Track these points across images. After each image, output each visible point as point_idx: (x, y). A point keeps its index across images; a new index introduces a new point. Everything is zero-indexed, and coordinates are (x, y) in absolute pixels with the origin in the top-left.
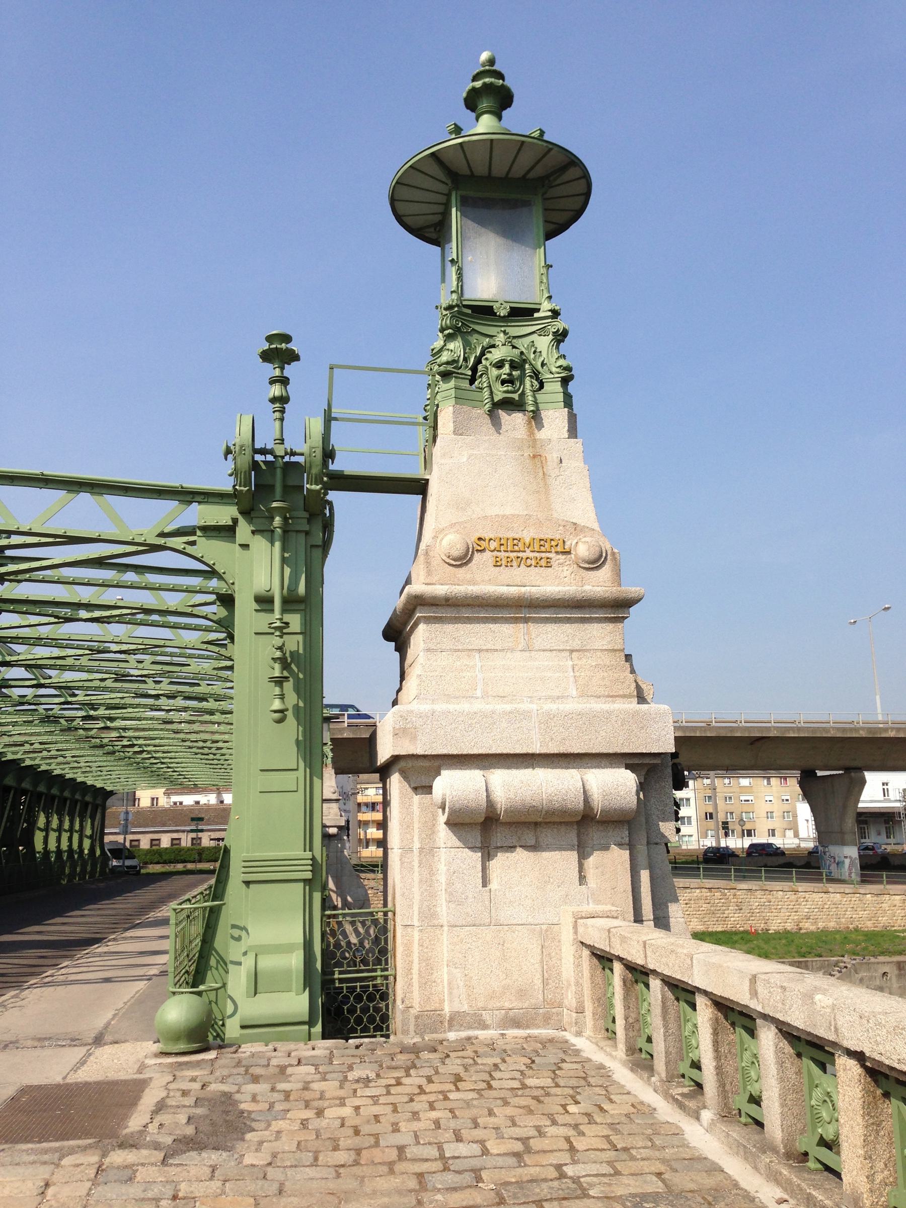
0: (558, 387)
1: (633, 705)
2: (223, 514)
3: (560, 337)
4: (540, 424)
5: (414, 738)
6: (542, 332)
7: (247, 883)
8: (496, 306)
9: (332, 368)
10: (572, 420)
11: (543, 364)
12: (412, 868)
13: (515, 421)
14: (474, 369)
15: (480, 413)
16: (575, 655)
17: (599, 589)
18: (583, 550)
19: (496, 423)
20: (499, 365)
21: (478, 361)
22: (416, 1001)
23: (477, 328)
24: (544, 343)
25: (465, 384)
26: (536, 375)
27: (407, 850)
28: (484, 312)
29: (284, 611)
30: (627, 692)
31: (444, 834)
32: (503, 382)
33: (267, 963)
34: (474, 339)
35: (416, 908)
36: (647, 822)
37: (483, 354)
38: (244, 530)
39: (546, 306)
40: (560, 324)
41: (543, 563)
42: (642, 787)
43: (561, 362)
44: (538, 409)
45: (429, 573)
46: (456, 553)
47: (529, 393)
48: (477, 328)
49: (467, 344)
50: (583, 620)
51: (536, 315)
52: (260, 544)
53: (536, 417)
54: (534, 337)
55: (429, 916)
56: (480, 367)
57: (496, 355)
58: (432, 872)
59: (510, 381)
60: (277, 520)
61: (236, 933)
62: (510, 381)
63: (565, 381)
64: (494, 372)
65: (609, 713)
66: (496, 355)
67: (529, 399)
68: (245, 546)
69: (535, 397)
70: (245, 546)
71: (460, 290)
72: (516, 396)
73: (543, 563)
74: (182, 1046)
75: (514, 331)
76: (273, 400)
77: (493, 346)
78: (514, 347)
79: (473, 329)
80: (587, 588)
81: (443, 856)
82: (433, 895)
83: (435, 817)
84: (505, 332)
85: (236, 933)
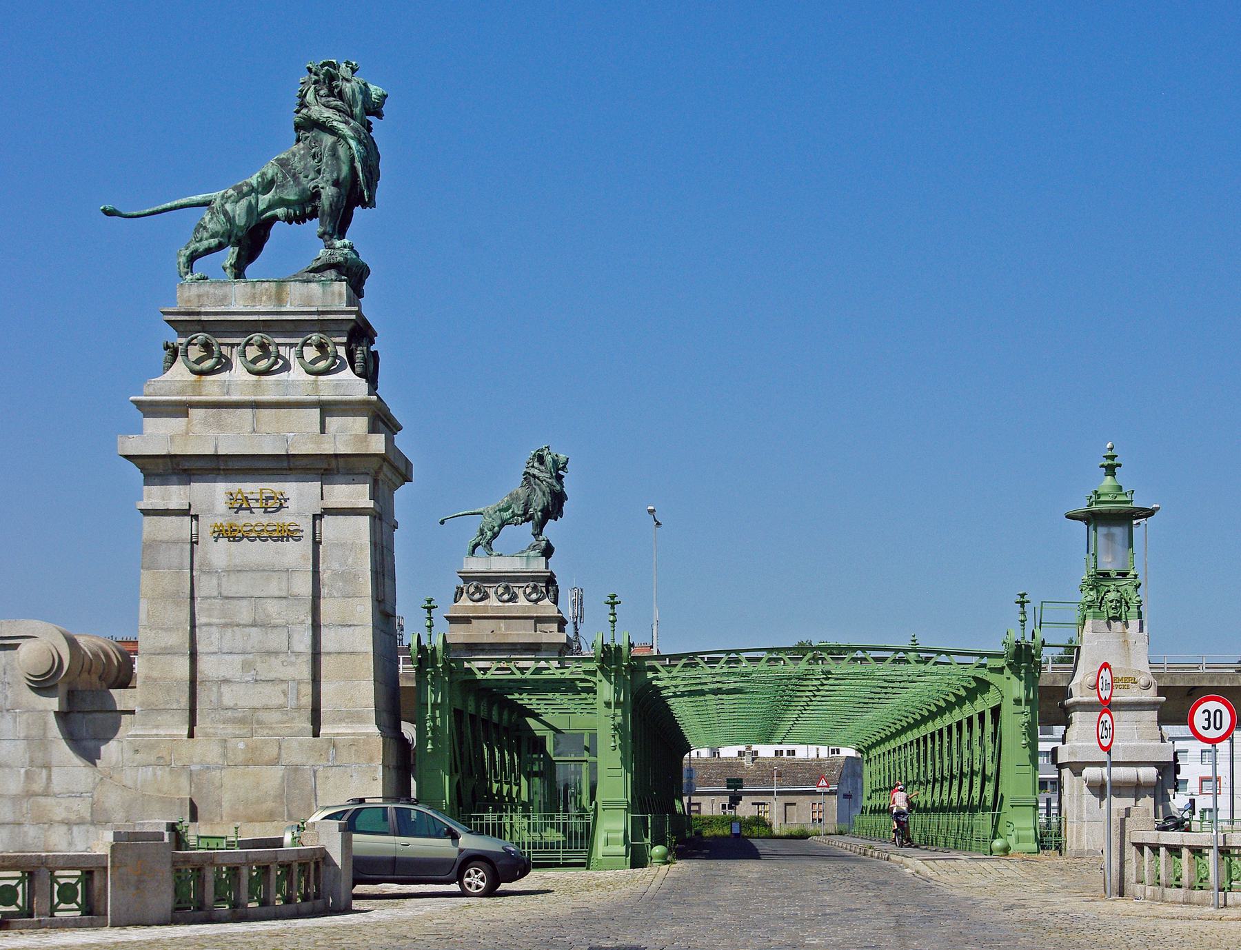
0: (1136, 610)
1: (1159, 743)
2: (1000, 663)
3: (1137, 587)
4: (1127, 627)
5: (1076, 756)
6: (1130, 584)
7: (1012, 806)
8: (1111, 572)
9: (1042, 603)
10: (1141, 624)
11: (1130, 599)
12: (1073, 802)
13: (1117, 626)
14: (1101, 603)
15: (1103, 622)
16: (1137, 723)
17: (1147, 698)
18: (1142, 682)
19: (1109, 626)
20: (1112, 601)
21: (1103, 599)
22: (1074, 847)
23: (1102, 583)
24: (1131, 589)
25: (1097, 610)
26: (1127, 603)
27: (1071, 795)
28: (1106, 575)
29: (1026, 705)
30: (1157, 738)
31: (1086, 789)
32: (1113, 609)
33: (1021, 833)
34: (1100, 589)
35: (1075, 816)
36: (1162, 788)
37: (1105, 595)
38: (1007, 672)
39: (1132, 572)
40: (1138, 581)
41: (1126, 687)
42: (1160, 774)
43: (1138, 599)
44: (1127, 619)
45: (1081, 692)
46: (1092, 684)
47: (1123, 613)
48: (1102, 583)
49: (1098, 591)
50: (1141, 710)
51: (1128, 576)
52: (1014, 678)
53: (1126, 625)
54: (1127, 586)
55: (1080, 818)
56: (1103, 602)
57: (1111, 596)
58: (1081, 803)
59: (1116, 608)
60: (1023, 671)
61: (1008, 824)
62: (1116, 608)
63: (1139, 607)
64: (1110, 604)
65: (1149, 746)
66: (1111, 596)
67: (1124, 616)
68: (1008, 678)
69: (1126, 615)
70: (1008, 678)
71: (1096, 568)
72: (1118, 615)
73: (1126, 687)
74: (1002, 853)
75: (1118, 583)
76: (1021, 621)
77: (1109, 591)
78: (1118, 591)
79: (1101, 585)
80: (1143, 697)
81: (1085, 797)
82: (1081, 811)
83: (1082, 783)
84: (1114, 585)
85: (1008, 824)
